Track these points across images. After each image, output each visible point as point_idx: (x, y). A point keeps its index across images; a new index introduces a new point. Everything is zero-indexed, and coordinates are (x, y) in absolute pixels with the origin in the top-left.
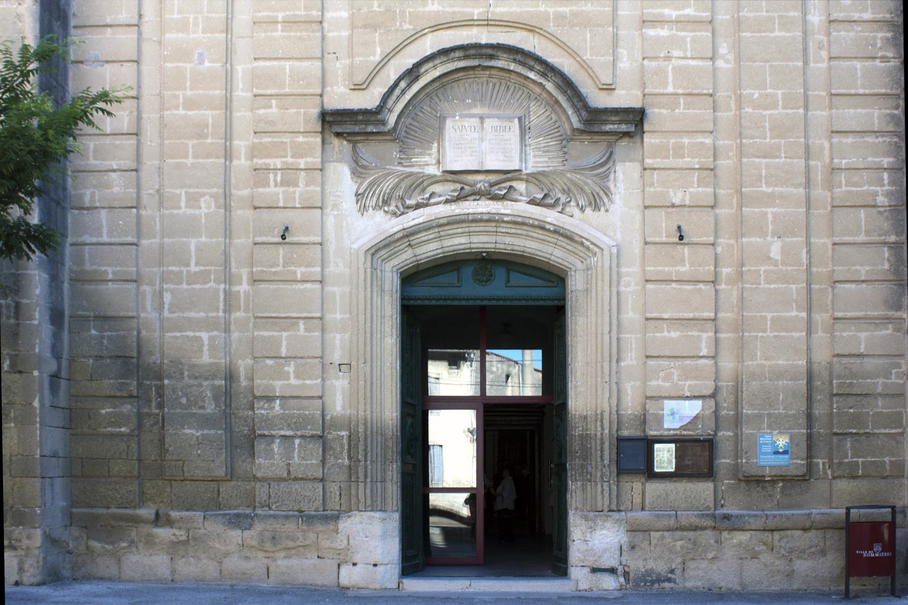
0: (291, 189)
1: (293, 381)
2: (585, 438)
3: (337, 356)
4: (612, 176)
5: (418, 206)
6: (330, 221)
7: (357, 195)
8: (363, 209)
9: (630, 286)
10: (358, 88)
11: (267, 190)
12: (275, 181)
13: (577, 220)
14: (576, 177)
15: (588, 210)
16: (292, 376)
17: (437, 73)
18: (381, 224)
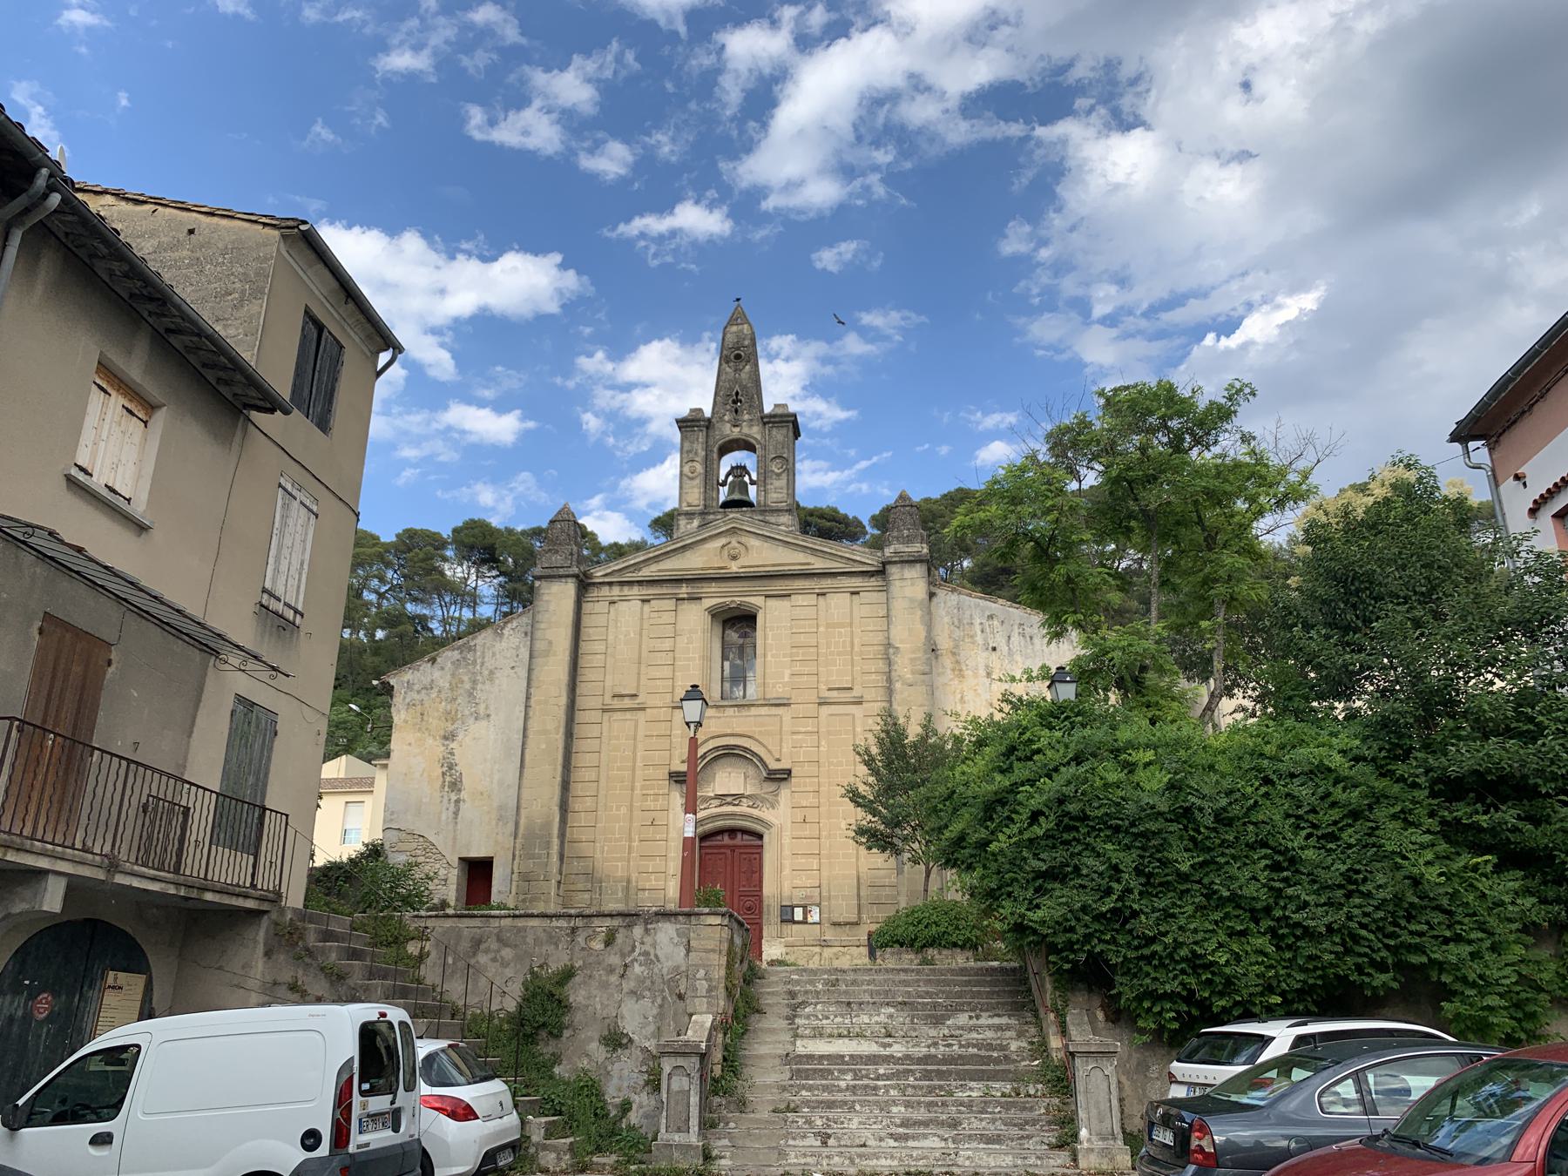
9: (786, 841)
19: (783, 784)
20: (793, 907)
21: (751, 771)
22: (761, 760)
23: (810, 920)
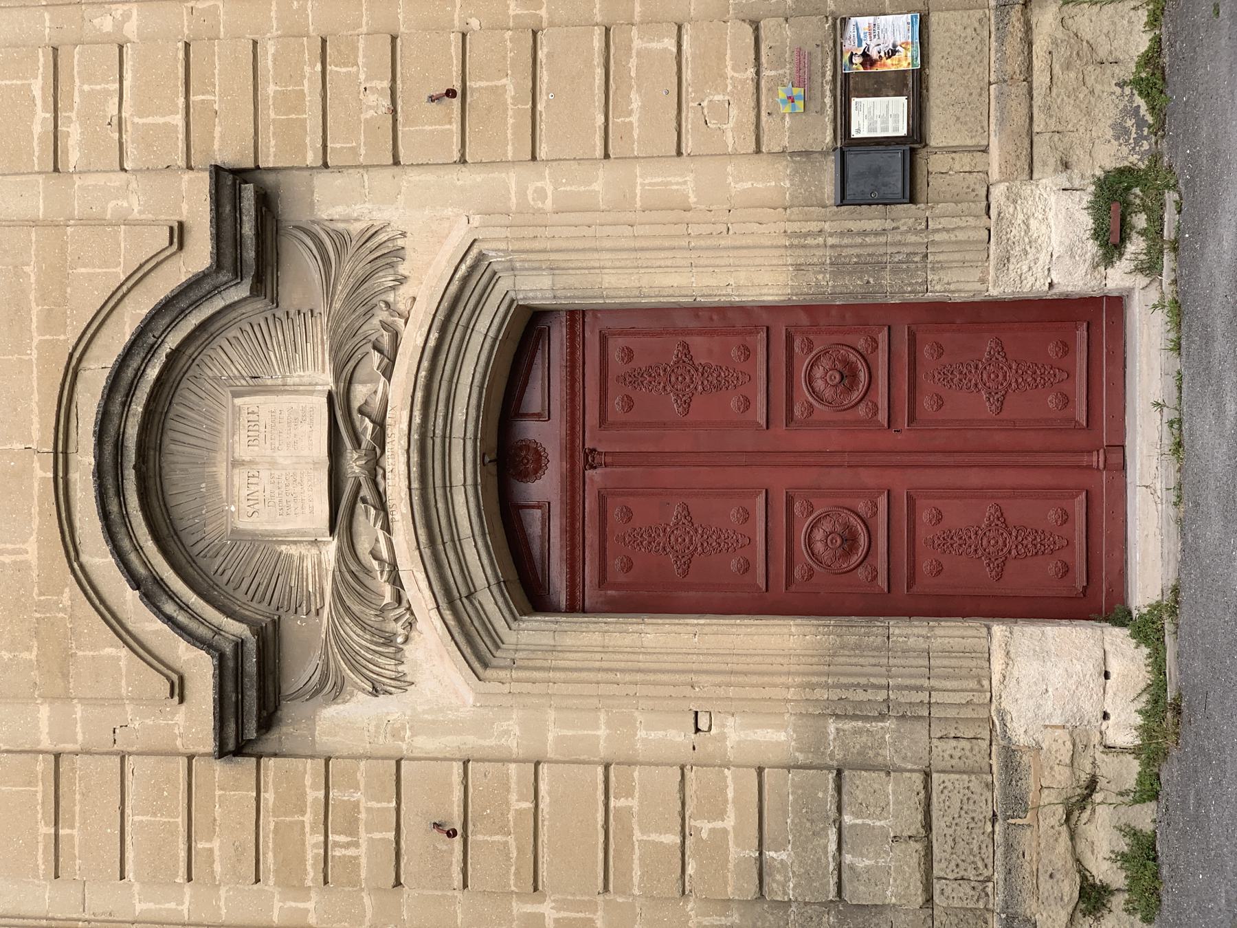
0: (363, 816)
1: (729, 822)
2: (838, 267)
3: (679, 737)
4: (340, 226)
5: (395, 580)
6: (425, 744)
7: (375, 692)
8: (402, 682)
10: (178, 689)
11: (363, 861)
12: (347, 846)
13: (420, 291)
14: (341, 291)
15: (403, 269)
16: (719, 824)
17: (149, 546)
18: (430, 646)
19: (292, 212)
20: (848, 146)
21: (226, 361)
22: (170, 308)
23: (905, 61)
